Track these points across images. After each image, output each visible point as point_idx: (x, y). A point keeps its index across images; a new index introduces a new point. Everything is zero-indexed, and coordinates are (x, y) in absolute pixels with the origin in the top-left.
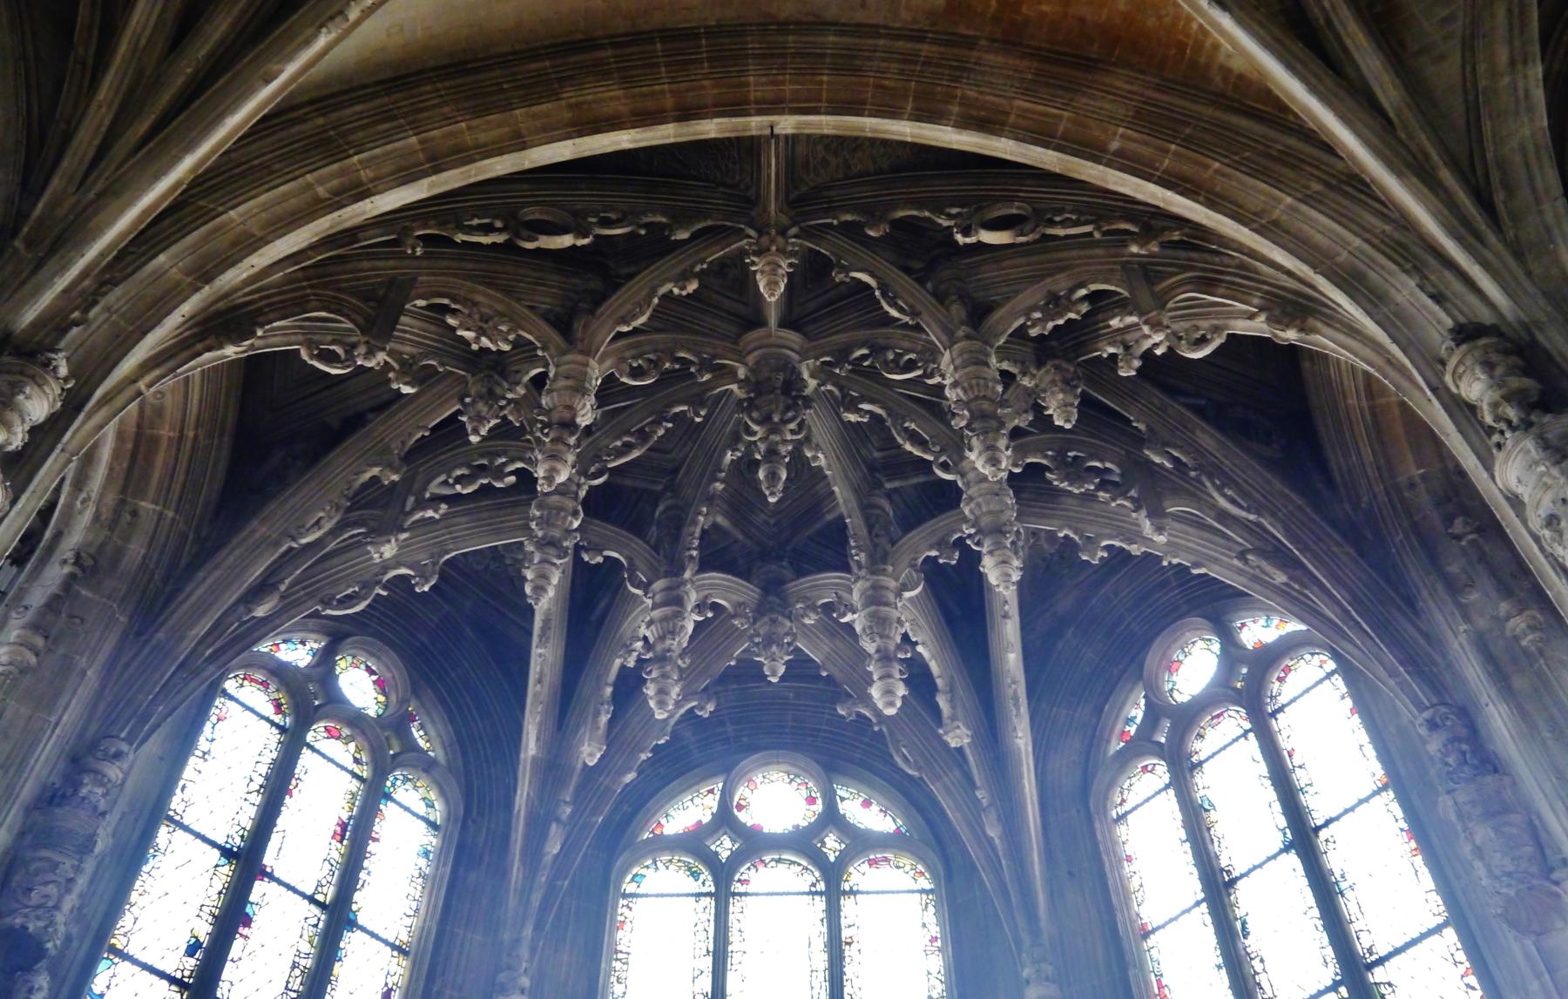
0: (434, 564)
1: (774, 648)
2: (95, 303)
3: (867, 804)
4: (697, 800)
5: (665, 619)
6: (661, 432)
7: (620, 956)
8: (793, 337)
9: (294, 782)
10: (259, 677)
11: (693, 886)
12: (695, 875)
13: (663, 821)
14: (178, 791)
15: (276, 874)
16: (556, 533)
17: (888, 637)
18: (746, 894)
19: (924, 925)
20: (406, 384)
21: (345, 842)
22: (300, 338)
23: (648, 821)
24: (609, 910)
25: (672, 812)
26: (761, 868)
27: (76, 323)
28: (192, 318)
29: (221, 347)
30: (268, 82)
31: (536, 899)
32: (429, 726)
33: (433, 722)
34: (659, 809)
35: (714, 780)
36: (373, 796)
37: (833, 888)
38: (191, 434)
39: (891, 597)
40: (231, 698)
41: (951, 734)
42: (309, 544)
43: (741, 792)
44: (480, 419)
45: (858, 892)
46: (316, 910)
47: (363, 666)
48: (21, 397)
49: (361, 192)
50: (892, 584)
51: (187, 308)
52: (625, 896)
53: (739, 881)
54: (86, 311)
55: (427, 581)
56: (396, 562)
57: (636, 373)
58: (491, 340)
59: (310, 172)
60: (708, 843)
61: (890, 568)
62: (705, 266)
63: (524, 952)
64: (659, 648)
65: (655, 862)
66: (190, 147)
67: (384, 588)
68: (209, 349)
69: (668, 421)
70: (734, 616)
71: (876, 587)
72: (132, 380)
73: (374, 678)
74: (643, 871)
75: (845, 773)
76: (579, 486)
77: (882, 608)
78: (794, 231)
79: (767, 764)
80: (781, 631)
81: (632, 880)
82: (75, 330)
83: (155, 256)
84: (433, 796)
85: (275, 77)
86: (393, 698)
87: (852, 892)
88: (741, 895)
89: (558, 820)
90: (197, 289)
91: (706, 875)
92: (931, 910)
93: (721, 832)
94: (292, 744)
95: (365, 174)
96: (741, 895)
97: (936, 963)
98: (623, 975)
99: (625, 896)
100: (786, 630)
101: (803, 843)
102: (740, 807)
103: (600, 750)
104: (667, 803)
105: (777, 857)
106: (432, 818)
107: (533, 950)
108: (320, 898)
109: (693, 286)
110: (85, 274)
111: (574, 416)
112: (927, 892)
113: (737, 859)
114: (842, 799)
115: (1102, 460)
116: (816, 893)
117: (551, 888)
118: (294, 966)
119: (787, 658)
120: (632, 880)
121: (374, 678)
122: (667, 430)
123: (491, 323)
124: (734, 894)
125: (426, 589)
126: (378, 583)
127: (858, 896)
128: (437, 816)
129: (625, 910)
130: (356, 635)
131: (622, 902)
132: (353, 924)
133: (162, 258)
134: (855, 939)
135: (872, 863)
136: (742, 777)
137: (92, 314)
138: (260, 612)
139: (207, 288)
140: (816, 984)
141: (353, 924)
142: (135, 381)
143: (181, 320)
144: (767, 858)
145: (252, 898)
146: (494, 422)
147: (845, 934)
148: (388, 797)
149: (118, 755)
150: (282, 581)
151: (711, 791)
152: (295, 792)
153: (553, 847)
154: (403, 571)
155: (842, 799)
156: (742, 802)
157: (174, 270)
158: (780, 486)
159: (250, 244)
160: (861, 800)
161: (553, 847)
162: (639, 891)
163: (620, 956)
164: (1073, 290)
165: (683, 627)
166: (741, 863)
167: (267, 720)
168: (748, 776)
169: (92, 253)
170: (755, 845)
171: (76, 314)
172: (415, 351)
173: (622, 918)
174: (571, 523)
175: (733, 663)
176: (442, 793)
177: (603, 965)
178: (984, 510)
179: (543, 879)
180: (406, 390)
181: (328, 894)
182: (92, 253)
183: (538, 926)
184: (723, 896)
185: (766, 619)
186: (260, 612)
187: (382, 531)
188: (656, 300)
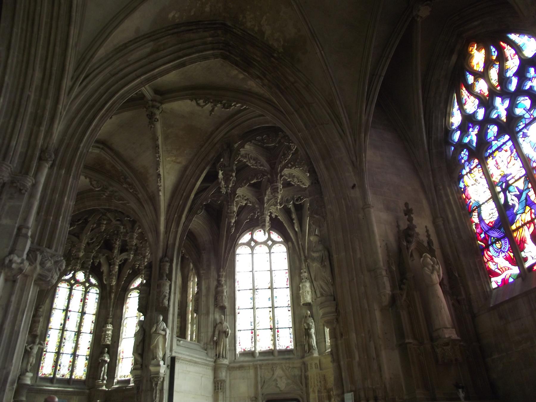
10: (64, 282)
31: (112, 304)
36: (86, 292)
63: (111, 312)
81: (130, 295)
94: (71, 289)
106: (97, 293)
108: (79, 311)
118: (77, 322)
128: (98, 292)
132: (85, 313)
146: (75, 250)
149: (41, 307)
179: (112, 300)
181: (81, 310)
183: (113, 307)
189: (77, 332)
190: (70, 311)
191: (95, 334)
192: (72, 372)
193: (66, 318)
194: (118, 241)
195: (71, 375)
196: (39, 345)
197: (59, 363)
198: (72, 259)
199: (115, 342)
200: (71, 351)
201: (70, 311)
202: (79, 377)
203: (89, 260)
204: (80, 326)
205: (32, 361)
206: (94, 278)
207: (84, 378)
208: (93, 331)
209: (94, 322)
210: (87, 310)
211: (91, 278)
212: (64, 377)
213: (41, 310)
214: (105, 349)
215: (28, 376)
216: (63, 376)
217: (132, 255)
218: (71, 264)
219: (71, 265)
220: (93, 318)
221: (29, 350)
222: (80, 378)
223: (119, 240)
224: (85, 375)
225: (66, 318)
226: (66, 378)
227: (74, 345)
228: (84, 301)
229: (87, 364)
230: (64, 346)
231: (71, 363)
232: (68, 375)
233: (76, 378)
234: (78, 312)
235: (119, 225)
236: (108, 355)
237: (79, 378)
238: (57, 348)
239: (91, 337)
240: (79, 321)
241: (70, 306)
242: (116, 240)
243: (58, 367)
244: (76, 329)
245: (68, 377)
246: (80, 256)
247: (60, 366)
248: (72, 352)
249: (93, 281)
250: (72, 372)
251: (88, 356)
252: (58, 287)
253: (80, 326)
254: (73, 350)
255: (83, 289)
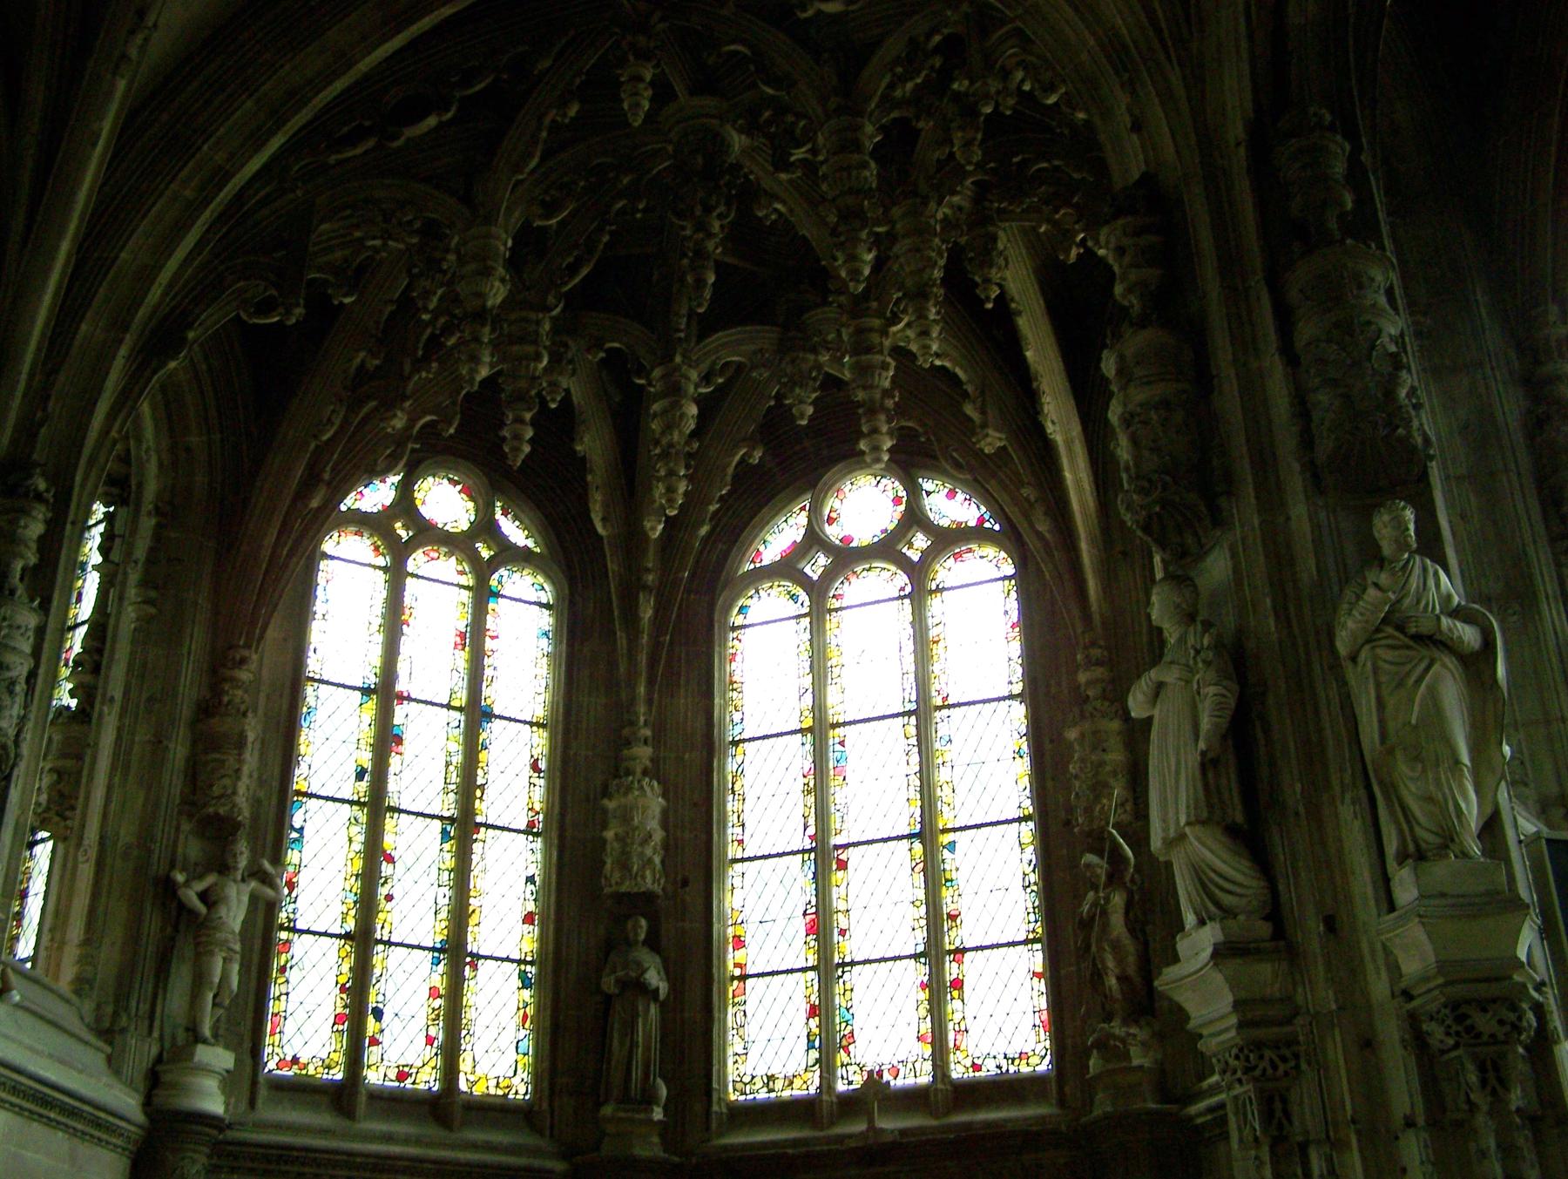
0: (454, 403)
1: (797, 390)
2: (48, 397)
3: (951, 495)
4: (791, 521)
5: (665, 412)
6: (606, 238)
7: (735, 686)
8: (710, 103)
9: (407, 612)
11: (793, 609)
12: (794, 598)
13: (762, 548)
14: (311, 653)
15: (413, 696)
16: (523, 384)
17: (871, 387)
18: (841, 609)
19: (1006, 612)
20: (346, 295)
21: (467, 649)
22: (234, 304)
23: (747, 549)
24: (717, 649)
25: (768, 538)
26: (853, 579)
27: (41, 425)
28: (130, 356)
29: (165, 364)
30: (94, 145)
31: (643, 659)
32: (522, 516)
33: (523, 511)
34: (755, 537)
35: (801, 499)
36: (483, 595)
37: (920, 590)
38: (204, 367)
39: (875, 338)
40: (332, 558)
41: (983, 443)
42: (329, 440)
43: (832, 503)
44: (427, 294)
45: (944, 589)
46: (456, 715)
47: (445, 481)
48: (20, 530)
49: (221, 176)
50: (877, 323)
51: (123, 351)
52: (734, 629)
53: (834, 596)
54: (45, 409)
55: (450, 424)
56: (412, 421)
57: (550, 209)
58: (397, 240)
59: (171, 182)
60: (800, 566)
61: (875, 305)
62: (584, 77)
63: (642, 709)
64: (664, 441)
65: (757, 591)
66: (60, 236)
67: (416, 440)
68: (155, 372)
69: (611, 225)
70: (754, 367)
71: (860, 331)
72: (105, 432)
73: (459, 487)
74: (749, 602)
75: (925, 467)
76: (538, 323)
77: (864, 358)
78: (657, 15)
79: (850, 472)
80: (805, 367)
81: (740, 612)
82: (43, 430)
83: (78, 328)
84: (540, 579)
85: (98, 136)
86: (480, 501)
87: (939, 590)
88: (836, 610)
89: (645, 587)
90: (121, 341)
91: (803, 597)
92: (1014, 595)
93: (813, 551)
94: (397, 576)
95: (220, 157)
96: (836, 610)
97: (1015, 648)
98: (739, 704)
99: (734, 629)
100: (811, 364)
101: (886, 549)
102: (831, 521)
103: (660, 522)
104: (762, 529)
105: (867, 566)
106: (544, 601)
107: (650, 702)
108: (456, 703)
109: (573, 110)
110: (31, 375)
111: (485, 302)
112: (1009, 578)
113: (829, 575)
114: (928, 493)
115: (1049, 161)
116: (905, 597)
117: (656, 646)
118: (448, 764)
119: (814, 396)
120: (740, 612)
121: (459, 487)
122: (611, 233)
123: (394, 221)
124: (830, 611)
125: (452, 431)
126: (409, 438)
127: (945, 593)
128: (547, 596)
129: (736, 642)
130: (428, 458)
131: (732, 635)
132: (489, 715)
133: (83, 327)
134: (942, 637)
135: (957, 556)
136: (829, 489)
137: (50, 409)
138: (314, 504)
139: (128, 336)
140: (908, 687)
141: (489, 715)
142: (108, 432)
143: (123, 361)
144: (859, 569)
145: (396, 722)
146: (440, 292)
147: (933, 633)
148: (498, 595)
149: (243, 661)
150: (323, 470)
151: (803, 509)
152: (411, 621)
153: (647, 613)
154: (428, 418)
155: (928, 493)
156: (834, 515)
157: (98, 331)
158: (708, 294)
159: (146, 276)
160: (946, 490)
161: (647, 613)
162: (746, 622)
163: (735, 686)
164: (929, 36)
165: (682, 415)
166: (833, 580)
167: (370, 565)
168: (837, 486)
169: (29, 357)
170: (847, 558)
171: (39, 414)
172: (347, 252)
173: (733, 651)
174: (535, 369)
175: (772, 403)
176: (548, 577)
177: (717, 701)
178: (907, 269)
179: (645, 639)
180: (347, 300)
181: (461, 699)
182: (29, 357)
183: (651, 682)
184: (818, 614)
185: (788, 359)
186: (314, 504)
187: (389, 405)
188: (544, 134)
189: (451, 820)
190: (402, 698)
191: (561, 837)
192: (450, 1053)
193: (386, 740)
194: (720, 217)
195: (450, 1070)
196: (253, 884)
197: (373, 1000)
198: (407, 368)
199: (685, 883)
200: (432, 931)
201: (402, 698)
202: (493, 1083)
203: (531, 349)
204: (468, 787)
205: (225, 977)
206: (516, 518)
207: (520, 1088)
208: (541, 817)
209: (543, 765)
210: (496, 695)
211: (498, 515)
212: (408, 1083)
213: (244, 675)
214: (636, 927)
215: (207, 1070)
216: (402, 1076)
217: (870, 250)
218: (404, 398)
219: (407, 404)
220: (540, 742)
221: (202, 909)
222: (500, 1092)
223: (722, 209)
224: (523, 1075)
225: (386, 740)
226: (421, 1086)
227: (444, 896)
228: (475, 639)
229: (530, 1011)
230: (389, 898)
231: (438, 1002)
232: (428, 1069)
233: (478, 1090)
234: (449, 707)
235: (716, 122)
236: (658, 959)
237: (492, 1091)
238: (353, 912)
239: (539, 856)
240: (458, 759)
241: (402, 667)
242: (708, 210)
243: (371, 1025)
244: (447, 805)
245: (427, 1079)
246: (490, 303)
247: (378, 1014)
248: (439, 938)
249: (515, 533)
250: (450, 1053)
251: (531, 963)
252: (326, 556)
253: (468, 787)
254: (444, 924)
255: (462, 573)
